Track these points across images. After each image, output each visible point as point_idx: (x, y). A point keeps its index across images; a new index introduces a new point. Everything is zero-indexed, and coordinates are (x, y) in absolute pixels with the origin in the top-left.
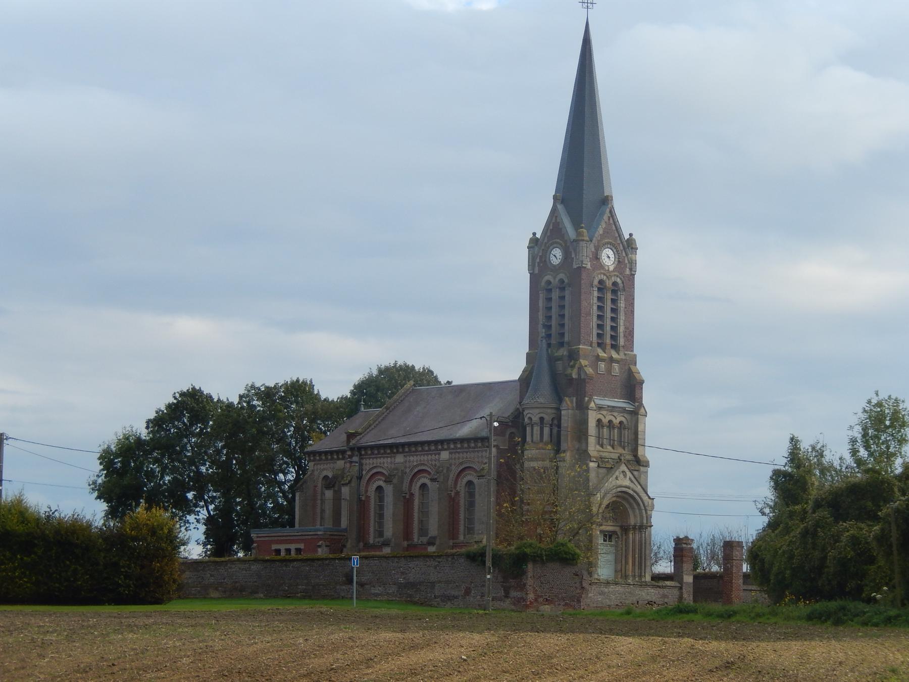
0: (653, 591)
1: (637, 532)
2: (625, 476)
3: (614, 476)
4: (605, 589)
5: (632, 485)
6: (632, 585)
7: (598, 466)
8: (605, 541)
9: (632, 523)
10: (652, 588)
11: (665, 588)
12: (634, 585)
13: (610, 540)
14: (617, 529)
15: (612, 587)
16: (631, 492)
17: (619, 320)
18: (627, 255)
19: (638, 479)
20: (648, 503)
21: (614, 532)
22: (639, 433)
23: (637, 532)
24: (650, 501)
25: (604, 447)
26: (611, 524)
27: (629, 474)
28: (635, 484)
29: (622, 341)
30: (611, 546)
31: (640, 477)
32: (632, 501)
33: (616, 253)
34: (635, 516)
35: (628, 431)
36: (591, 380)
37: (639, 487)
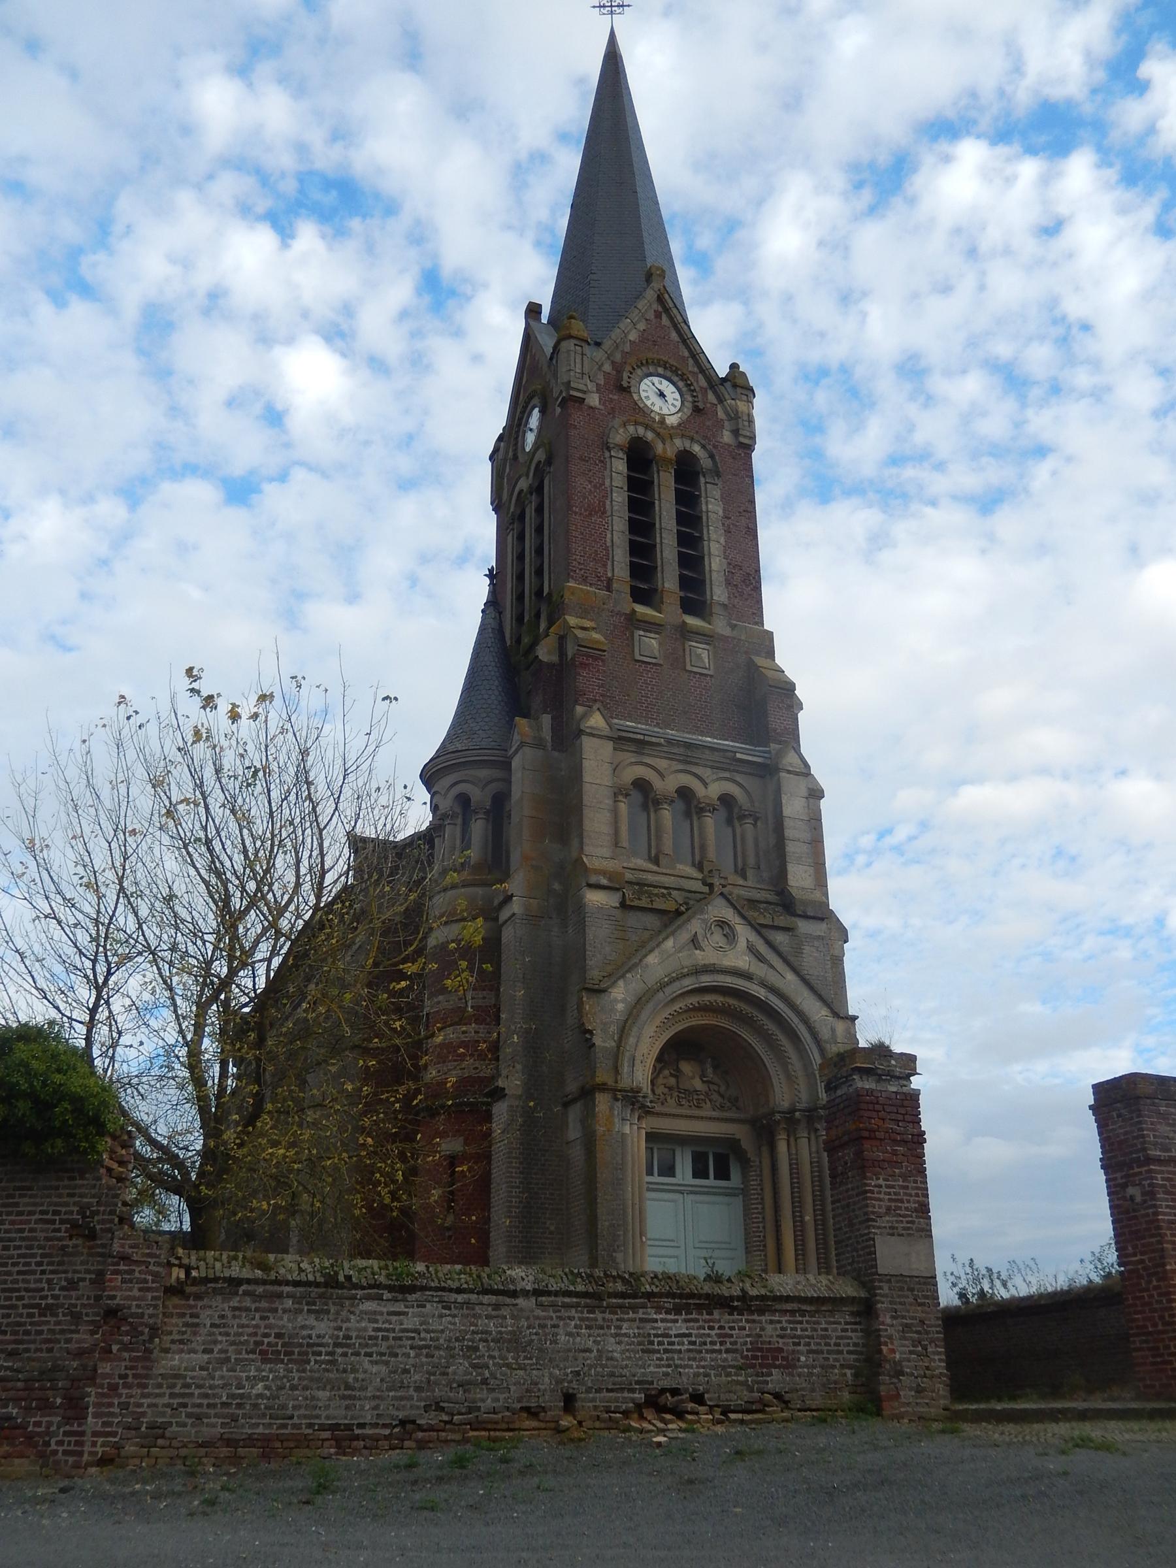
0: (681, 1327)
1: (803, 1133)
2: (731, 936)
3: (684, 936)
5: (759, 970)
6: (526, 1293)
7: (623, 905)
8: (700, 1172)
9: (786, 1105)
10: (677, 1310)
11: (761, 1312)
12: (537, 1293)
13: (723, 1173)
14: (738, 1131)
15: (369, 1306)
16: (761, 993)
17: (705, 543)
18: (721, 400)
19: (791, 959)
20: (833, 1030)
21: (733, 1144)
22: (787, 823)
23: (803, 1133)
24: (840, 1027)
25: (663, 861)
27: (744, 933)
28: (772, 967)
29: (718, 593)
30: (730, 1193)
31: (798, 951)
32: (770, 1026)
33: (684, 389)
34: (790, 1079)
35: (755, 825)
36: (596, 659)
37: (790, 976)
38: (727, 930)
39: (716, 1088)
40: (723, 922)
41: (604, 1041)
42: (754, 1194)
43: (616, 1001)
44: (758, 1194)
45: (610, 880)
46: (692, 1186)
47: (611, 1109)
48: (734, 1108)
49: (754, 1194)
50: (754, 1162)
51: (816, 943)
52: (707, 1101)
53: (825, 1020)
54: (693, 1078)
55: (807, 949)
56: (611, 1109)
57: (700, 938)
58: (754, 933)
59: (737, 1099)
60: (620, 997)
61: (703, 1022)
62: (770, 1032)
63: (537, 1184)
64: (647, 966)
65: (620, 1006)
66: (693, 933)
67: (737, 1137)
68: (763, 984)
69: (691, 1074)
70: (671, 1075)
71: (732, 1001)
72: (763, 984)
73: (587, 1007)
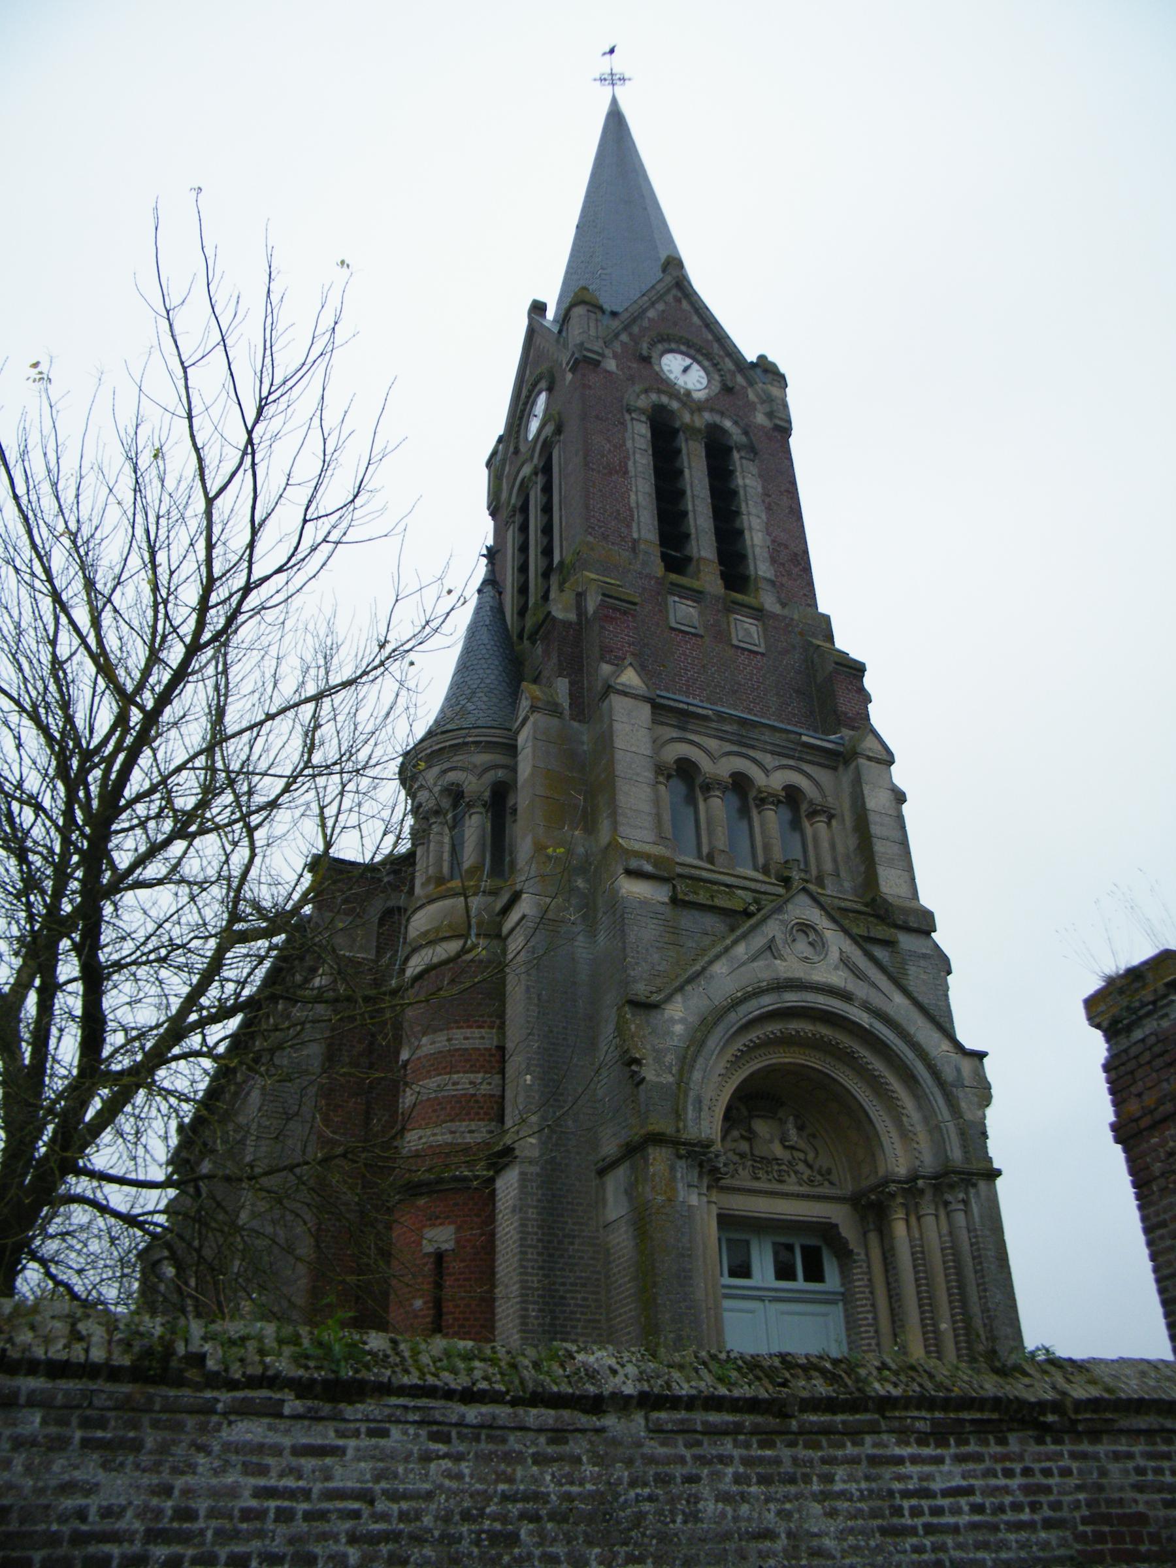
0: (949, 1475)
1: (927, 1208)
2: (819, 944)
3: (758, 941)
4: (90, 1470)
5: (860, 990)
6: (623, 1403)
7: (675, 901)
8: (784, 1272)
9: (902, 1171)
10: (939, 1436)
11: (1095, 1435)
12: (648, 1401)
13: (814, 1273)
14: (838, 1214)
15: (249, 1431)
16: (864, 1019)
17: (745, 517)
18: (751, 383)
20: (958, 1070)
21: (828, 1231)
22: (872, 817)
23: (927, 1208)
24: (966, 1065)
25: (720, 859)
26: (804, 1189)
27: (836, 942)
28: (874, 985)
29: (761, 567)
30: (827, 1299)
32: (878, 1065)
33: (711, 369)
34: (905, 1135)
35: (829, 824)
36: (625, 613)
37: (899, 998)
38: (812, 936)
39: (802, 1156)
40: (807, 926)
41: (658, 1075)
42: (861, 1299)
43: (672, 1021)
44: (866, 1299)
45: (655, 866)
46: (776, 1290)
47: (672, 1169)
48: (826, 1183)
49: (861, 1299)
50: (858, 1254)
51: (923, 963)
52: (792, 1174)
53: (947, 1057)
54: (771, 1141)
55: (912, 970)
56: (672, 1169)
57: (779, 942)
58: (849, 942)
59: (829, 1171)
60: (678, 1015)
61: (787, 1060)
62: (876, 1073)
63: (563, 1284)
64: (712, 977)
65: (678, 1028)
66: (770, 936)
67: (834, 1221)
68: (866, 1007)
69: (768, 1136)
70: (743, 1137)
71: (825, 1031)
72: (866, 1007)
73: (633, 1027)
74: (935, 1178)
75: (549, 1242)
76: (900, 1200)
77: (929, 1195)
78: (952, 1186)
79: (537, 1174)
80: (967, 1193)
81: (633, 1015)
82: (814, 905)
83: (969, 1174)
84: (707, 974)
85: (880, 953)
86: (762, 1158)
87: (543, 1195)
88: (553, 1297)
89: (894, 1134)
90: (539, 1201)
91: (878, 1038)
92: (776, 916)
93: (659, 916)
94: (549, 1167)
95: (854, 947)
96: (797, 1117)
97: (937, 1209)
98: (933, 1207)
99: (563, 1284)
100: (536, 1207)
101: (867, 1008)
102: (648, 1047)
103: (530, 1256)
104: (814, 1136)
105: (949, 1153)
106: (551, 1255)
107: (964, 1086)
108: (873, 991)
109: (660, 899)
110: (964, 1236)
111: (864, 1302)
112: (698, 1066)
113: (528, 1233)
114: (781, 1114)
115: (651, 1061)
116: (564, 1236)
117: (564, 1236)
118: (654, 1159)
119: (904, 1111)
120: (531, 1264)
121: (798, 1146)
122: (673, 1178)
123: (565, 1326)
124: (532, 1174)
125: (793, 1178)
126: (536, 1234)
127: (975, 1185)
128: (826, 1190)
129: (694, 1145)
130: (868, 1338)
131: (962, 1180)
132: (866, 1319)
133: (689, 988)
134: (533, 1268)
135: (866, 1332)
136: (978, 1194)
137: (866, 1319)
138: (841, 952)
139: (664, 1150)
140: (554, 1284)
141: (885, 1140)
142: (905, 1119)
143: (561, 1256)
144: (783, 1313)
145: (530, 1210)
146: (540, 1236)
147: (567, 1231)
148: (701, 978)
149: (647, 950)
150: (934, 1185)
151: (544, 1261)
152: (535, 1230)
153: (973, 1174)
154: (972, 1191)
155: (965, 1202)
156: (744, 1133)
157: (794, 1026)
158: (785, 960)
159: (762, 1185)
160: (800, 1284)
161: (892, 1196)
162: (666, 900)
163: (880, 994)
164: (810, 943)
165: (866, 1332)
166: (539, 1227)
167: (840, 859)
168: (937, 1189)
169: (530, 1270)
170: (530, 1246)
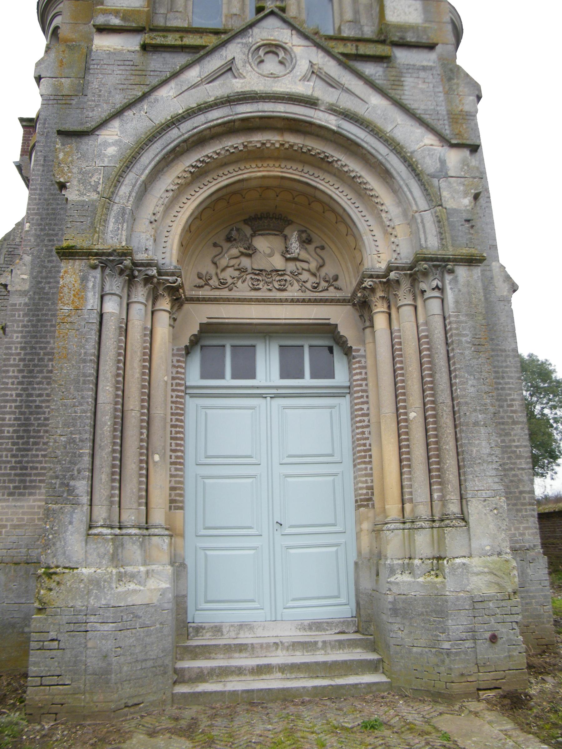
19: (392, 93)
20: (443, 162)
26: (309, 295)
31: (398, 83)
38: (282, 54)
39: (305, 266)
40: (277, 46)
41: (82, 194)
42: (358, 392)
43: (106, 144)
44: (363, 391)
45: (124, 19)
46: (277, 388)
47: (84, 279)
48: (332, 289)
49: (358, 392)
50: (358, 350)
51: (422, 74)
52: (296, 283)
53: (429, 150)
54: (271, 255)
55: (409, 81)
56: (84, 279)
57: (239, 63)
58: (321, 54)
59: (336, 278)
60: (111, 139)
61: (259, 174)
62: (353, 175)
63: (40, 395)
64: (156, 100)
65: (111, 150)
66: (229, 58)
67: (332, 322)
68: (333, 110)
69: (268, 251)
70: (242, 254)
71: (292, 139)
72: (333, 110)
73: (61, 156)
74: (411, 268)
75: (30, 360)
76: (380, 294)
77: (405, 285)
78: (425, 274)
79: (26, 304)
80: (443, 281)
81: (63, 145)
82: (284, 26)
83: (443, 260)
84: (152, 98)
85: (369, 69)
86: (261, 271)
87: (29, 321)
88: (30, 407)
89: (378, 233)
90: (24, 326)
91: (348, 139)
92: (239, 40)
93: (127, 63)
94: (37, 297)
95: (327, 58)
96: (301, 232)
97: (415, 299)
98: (411, 297)
99: (40, 395)
100: (22, 332)
101: (335, 111)
102: (75, 170)
103: (11, 374)
104: (323, 248)
105: (423, 242)
106: (31, 371)
107: (447, 176)
108: (345, 96)
109: (130, 49)
110: (437, 323)
111: (360, 394)
112: (127, 181)
113: (12, 354)
114: (286, 232)
115: (75, 183)
116: (45, 354)
117: (45, 354)
118: (66, 272)
119: (383, 208)
120: (10, 381)
121: (300, 257)
122: (84, 288)
123: (39, 431)
124: (20, 304)
125: (296, 286)
126: (19, 354)
127: (451, 271)
128: (332, 293)
129: (110, 254)
130: (362, 427)
131: (436, 267)
132: (362, 409)
133: (129, 114)
134: (13, 383)
135: (360, 421)
136: (455, 281)
137: (362, 409)
138: (312, 64)
139: (77, 262)
140: (31, 395)
141: (367, 239)
142: (383, 215)
143: (41, 372)
144: (285, 408)
145: (15, 335)
146: (22, 356)
147: (48, 349)
148: (146, 101)
149: (110, 92)
150: (411, 275)
151: (23, 377)
152: (18, 351)
153: (449, 260)
154: (448, 278)
155: (440, 289)
156: (242, 250)
157: (257, 139)
158: (244, 77)
159: (264, 294)
160: (307, 381)
161: (372, 290)
162: (138, 48)
163: (353, 98)
164: (281, 63)
165: (360, 421)
166: (22, 348)
167: (362, 9)
168: (414, 279)
169: (10, 386)
170: (12, 366)
